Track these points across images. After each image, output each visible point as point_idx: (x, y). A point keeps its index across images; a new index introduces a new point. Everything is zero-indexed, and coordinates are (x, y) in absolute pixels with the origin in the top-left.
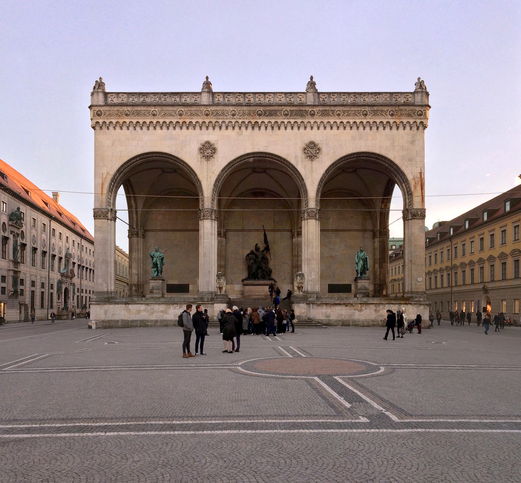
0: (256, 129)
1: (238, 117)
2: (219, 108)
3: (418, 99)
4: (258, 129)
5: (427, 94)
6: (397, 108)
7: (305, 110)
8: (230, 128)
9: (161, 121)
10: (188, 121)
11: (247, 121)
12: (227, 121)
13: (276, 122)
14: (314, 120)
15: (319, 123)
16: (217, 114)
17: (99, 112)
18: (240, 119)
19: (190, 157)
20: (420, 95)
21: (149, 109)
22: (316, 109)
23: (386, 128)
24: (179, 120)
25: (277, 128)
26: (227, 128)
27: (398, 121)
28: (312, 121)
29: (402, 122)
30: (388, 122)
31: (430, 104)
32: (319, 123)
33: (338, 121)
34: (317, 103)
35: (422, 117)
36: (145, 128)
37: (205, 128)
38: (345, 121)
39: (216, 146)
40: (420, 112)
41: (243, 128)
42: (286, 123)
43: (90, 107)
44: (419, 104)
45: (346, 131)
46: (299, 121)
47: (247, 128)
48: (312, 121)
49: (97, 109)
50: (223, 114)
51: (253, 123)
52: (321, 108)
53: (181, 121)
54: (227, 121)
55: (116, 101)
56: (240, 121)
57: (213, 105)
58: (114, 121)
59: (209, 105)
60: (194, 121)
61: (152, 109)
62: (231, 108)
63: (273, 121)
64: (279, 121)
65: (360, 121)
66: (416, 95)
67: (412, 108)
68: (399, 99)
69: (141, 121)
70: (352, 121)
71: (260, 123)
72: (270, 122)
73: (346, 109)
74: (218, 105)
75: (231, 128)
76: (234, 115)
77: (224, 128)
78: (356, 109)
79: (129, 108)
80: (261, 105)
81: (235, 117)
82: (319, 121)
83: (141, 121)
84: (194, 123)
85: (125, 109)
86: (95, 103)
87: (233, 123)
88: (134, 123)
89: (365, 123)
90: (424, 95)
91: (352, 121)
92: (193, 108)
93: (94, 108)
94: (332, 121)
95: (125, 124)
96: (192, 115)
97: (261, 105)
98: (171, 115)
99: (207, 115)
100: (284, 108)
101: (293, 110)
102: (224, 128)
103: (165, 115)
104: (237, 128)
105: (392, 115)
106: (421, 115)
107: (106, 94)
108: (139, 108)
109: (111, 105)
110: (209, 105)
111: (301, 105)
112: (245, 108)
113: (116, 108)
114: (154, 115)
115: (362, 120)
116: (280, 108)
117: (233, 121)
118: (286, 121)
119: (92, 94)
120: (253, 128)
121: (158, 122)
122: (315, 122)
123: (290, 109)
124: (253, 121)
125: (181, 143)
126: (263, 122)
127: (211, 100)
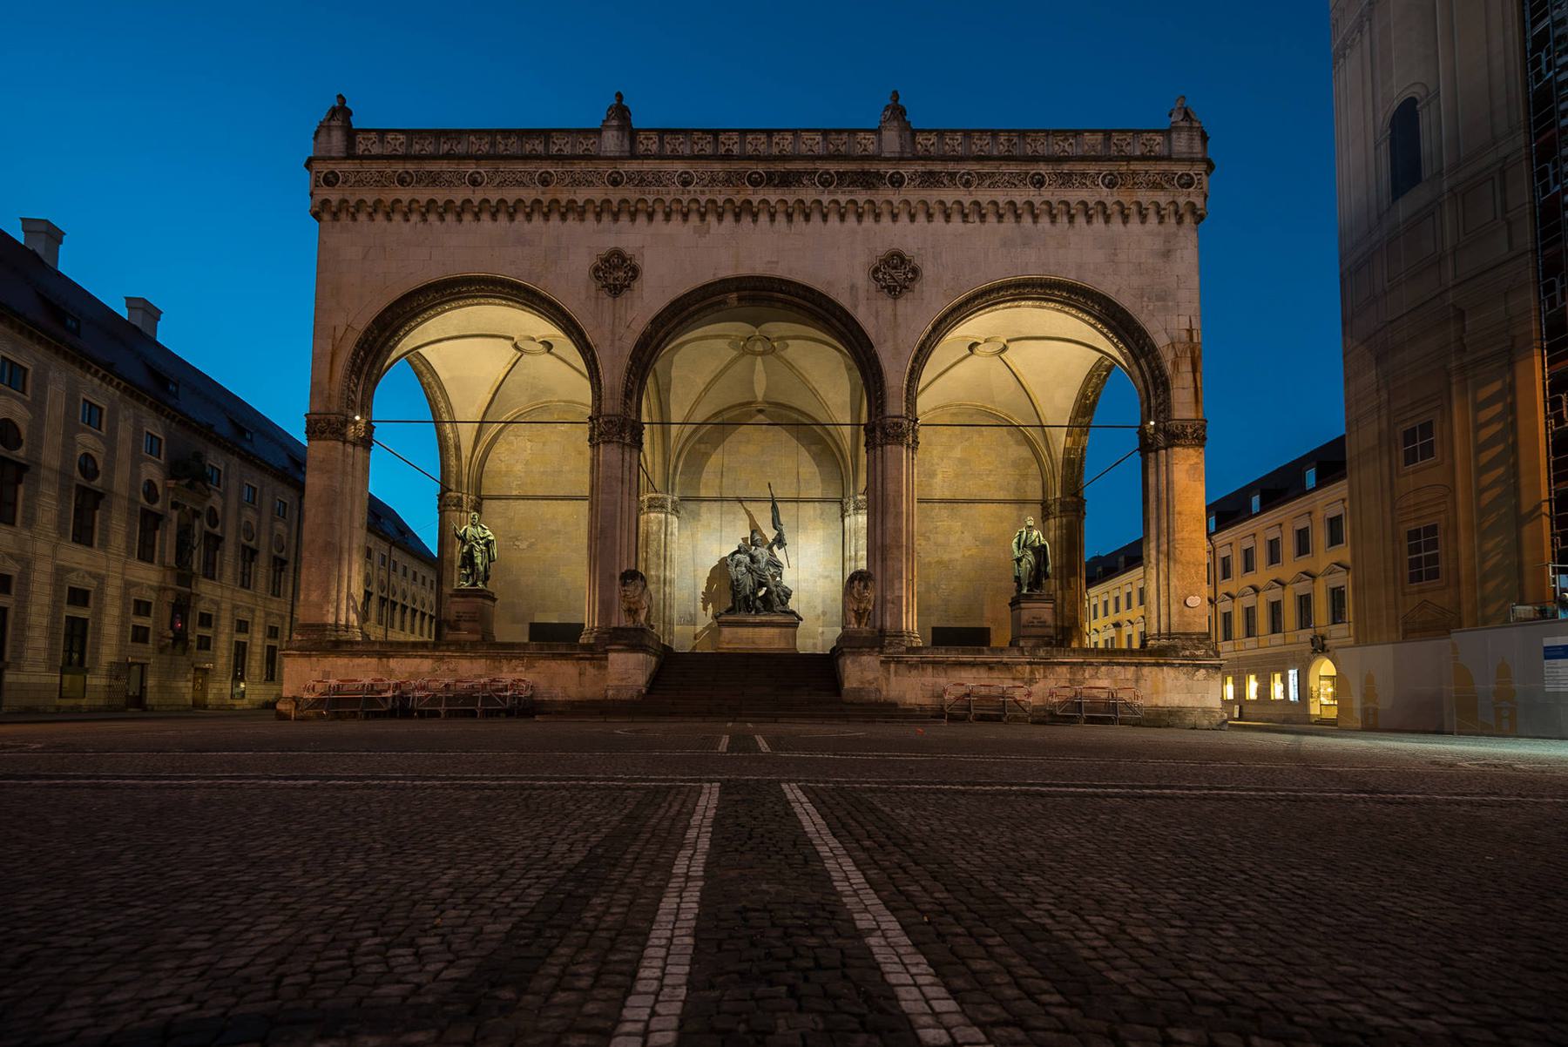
1: (699, 188)
2: (648, 166)
7: (878, 173)
8: (676, 219)
10: (564, 197)
11: (720, 199)
12: (668, 199)
16: (641, 180)
18: (703, 193)
19: (574, 291)
20: (1184, 135)
21: (462, 168)
22: (906, 170)
26: (668, 217)
31: (1210, 155)
36: (450, 218)
41: (711, 219)
43: (309, 164)
46: (861, 196)
48: (896, 197)
49: (324, 168)
50: (658, 179)
52: (919, 167)
53: (546, 199)
54: (668, 199)
56: (703, 199)
57: (633, 156)
59: (621, 158)
61: (470, 168)
62: (680, 167)
66: (1174, 136)
67: (1164, 166)
73: (986, 168)
74: (647, 157)
76: (686, 183)
77: (659, 217)
78: (1013, 168)
79: (411, 167)
80: (758, 158)
85: (399, 167)
92: (579, 167)
93: (317, 166)
96: (576, 183)
97: (758, 158)
98: (520, 184)
99: (615, 183)
100: (822, 166)
101: (845, 173)
102: (659, 217)
103: (501, 184)
104: (694, 219)
106: (1190, 185)
107: (351, 134)
109: (362, 158)
110: (621, 158)
112: (717, 167)
113: (375, 167)
114: (474, 183)
116: (810, 166)
117: (685, 198)
119: (317, 133)
120: (737, 217)
127: (627, 146)
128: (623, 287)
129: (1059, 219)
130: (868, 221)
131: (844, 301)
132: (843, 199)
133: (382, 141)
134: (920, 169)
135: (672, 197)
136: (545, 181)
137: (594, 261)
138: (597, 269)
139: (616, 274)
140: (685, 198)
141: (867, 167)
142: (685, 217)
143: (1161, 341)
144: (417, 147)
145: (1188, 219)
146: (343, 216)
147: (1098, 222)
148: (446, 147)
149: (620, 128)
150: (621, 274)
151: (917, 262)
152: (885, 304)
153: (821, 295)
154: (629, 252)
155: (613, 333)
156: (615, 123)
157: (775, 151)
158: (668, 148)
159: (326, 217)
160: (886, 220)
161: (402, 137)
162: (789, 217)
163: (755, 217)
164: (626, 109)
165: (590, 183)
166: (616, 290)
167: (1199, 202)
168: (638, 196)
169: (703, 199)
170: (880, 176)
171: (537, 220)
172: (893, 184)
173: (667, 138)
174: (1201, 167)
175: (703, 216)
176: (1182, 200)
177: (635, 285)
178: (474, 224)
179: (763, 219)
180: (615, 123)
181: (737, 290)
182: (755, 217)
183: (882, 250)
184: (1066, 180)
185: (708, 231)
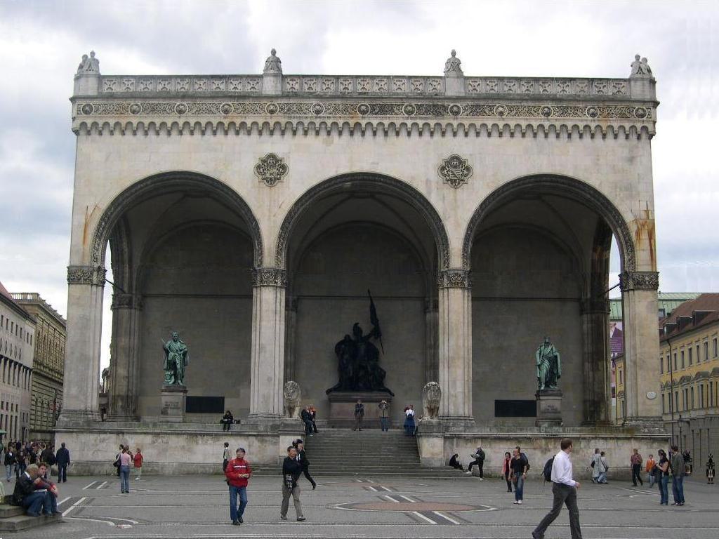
0: (357, 135)
2: (292, 101)
3: (637, 91)
4: (360, 134)
5: (653, 82)
6: (601, 105)
7: (443, 106)
8: (312, 133)
9: (192, 121)
11: (340, 122)
12: (306, 122)
13: (392, 124)
14: (459, 121)
15: (467, 127)
16: (288, 111)
17: (87, 108)
18: (329, 118)
20: (639, 83)
21: (172, 102)
23: (584, 136)
24: (223, 121)
25: (394, 134)
26: (306, 133)
27: (604, 125)
28: (455, 123)
29: (611, 127)
30: (586, 126)
31: (658, 100)
32: (467, 127)
33: (501, 124)
34: (463, 95)
35: (644, 119)
37: (268, 133)
38: (512, 124)
39: (286, 162)
40: (641, 112)
41: (335, 134)
42: (409, 126)
44: (639, 98)
45: (514, 140)
47: (340, 133)
51: (352, 126)
52: (470, 103)
54: (306, 122)
55: (118, 89)
56: (329, 122)
58: (112, 122)
59: (277, 97)
60: (249, 122)
62: (314, 102)
63: (386, 122)
64: (398, 122)
65: (538, 123)
66: (632, 83)
67: (624, 105)
68: (605, 90)
69: (158, 122)
70: (524, 124)
71: (363, 126)
72: (381, 124)
75: (314, 133)
76: (318, 112)
77: (300, 132)
81: (321, 115)
82: (467, 123)
83: (158, 122)
84: (249, 125)
86: (81, 94)
87: (317, 125)
88: (146, 124)
89: (546, 128)
90: (647, 83)
91: (524, 124)
93: (78, 102)
94: (490, 123)
95: (129, 127)
96: (245, 111)
97: (363, 95)
98: (210, 112)
99: (272, 112)
102: (300, 132)
103: (199, 112)
104: (323, 133)
105: (593, 115)
106: (643, 116)
107: (101, 78)
108: (155, 102)
111: (436, 97)
112: (338, 102)
113: (115, 102)
114: (181, 112)
115: (542, 123)
116: (399, 102)
117: (318, 122)
118: (409, 123)
119: (77, 78)
120: (352, 133)
121: (187, 123)
122: (461, 125)
123: (416, 103)
124: (352, 122)
125: (229, 160)
126: (369, 124)
127: (280, 88)
128: (276, 179)
129: (561, 136)
130: (437, 136)
131: (422, 189)
132: (421, 123)
133: (120, 83)
134: (470, 103)
135: (309, 120)
136: (226, 112)
137: (258, 162)
138: (258, 167)
139: (271, 169)
140: (318, 122)
141: (436, 102)
142: (317, 133)
143: (628, 218)
144: (142, 86)
145: (644, 136)
146: (93, 132)
147: (587, 138)
148: (160, 87)
149: (275, 75)
150: (275, 170)
151: (469, 163)
152: (448, 191)
153: (407, 186)
154: (280, 156)
155: (270, 211)
156: (272, 72)
157: (376, 88)
158: (306, 87)
159: (82, 133)
160: (449, 135)
161: (133, 80)
162: (386, 133)
163: (363, 133)
164: (278, 61)
165: (256, 112)
166: (271, 181)
167: (650, 126)
168: (287, 120)
169: (329, 122)
170: (445, 108)
171: (220, 135)
172: (452, 112)
173: (304, 80)
174: (650, 105)
175: (329, 133)
176: (639, 126)
177: (285, 178)
178: (179, 137)
179: (369, 133)
180: (272, 72)
181: (351, 180)
182: (363, 133)
183: (447, 155)
184: (564, 112)
185: (333, 141)
